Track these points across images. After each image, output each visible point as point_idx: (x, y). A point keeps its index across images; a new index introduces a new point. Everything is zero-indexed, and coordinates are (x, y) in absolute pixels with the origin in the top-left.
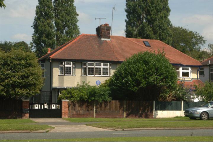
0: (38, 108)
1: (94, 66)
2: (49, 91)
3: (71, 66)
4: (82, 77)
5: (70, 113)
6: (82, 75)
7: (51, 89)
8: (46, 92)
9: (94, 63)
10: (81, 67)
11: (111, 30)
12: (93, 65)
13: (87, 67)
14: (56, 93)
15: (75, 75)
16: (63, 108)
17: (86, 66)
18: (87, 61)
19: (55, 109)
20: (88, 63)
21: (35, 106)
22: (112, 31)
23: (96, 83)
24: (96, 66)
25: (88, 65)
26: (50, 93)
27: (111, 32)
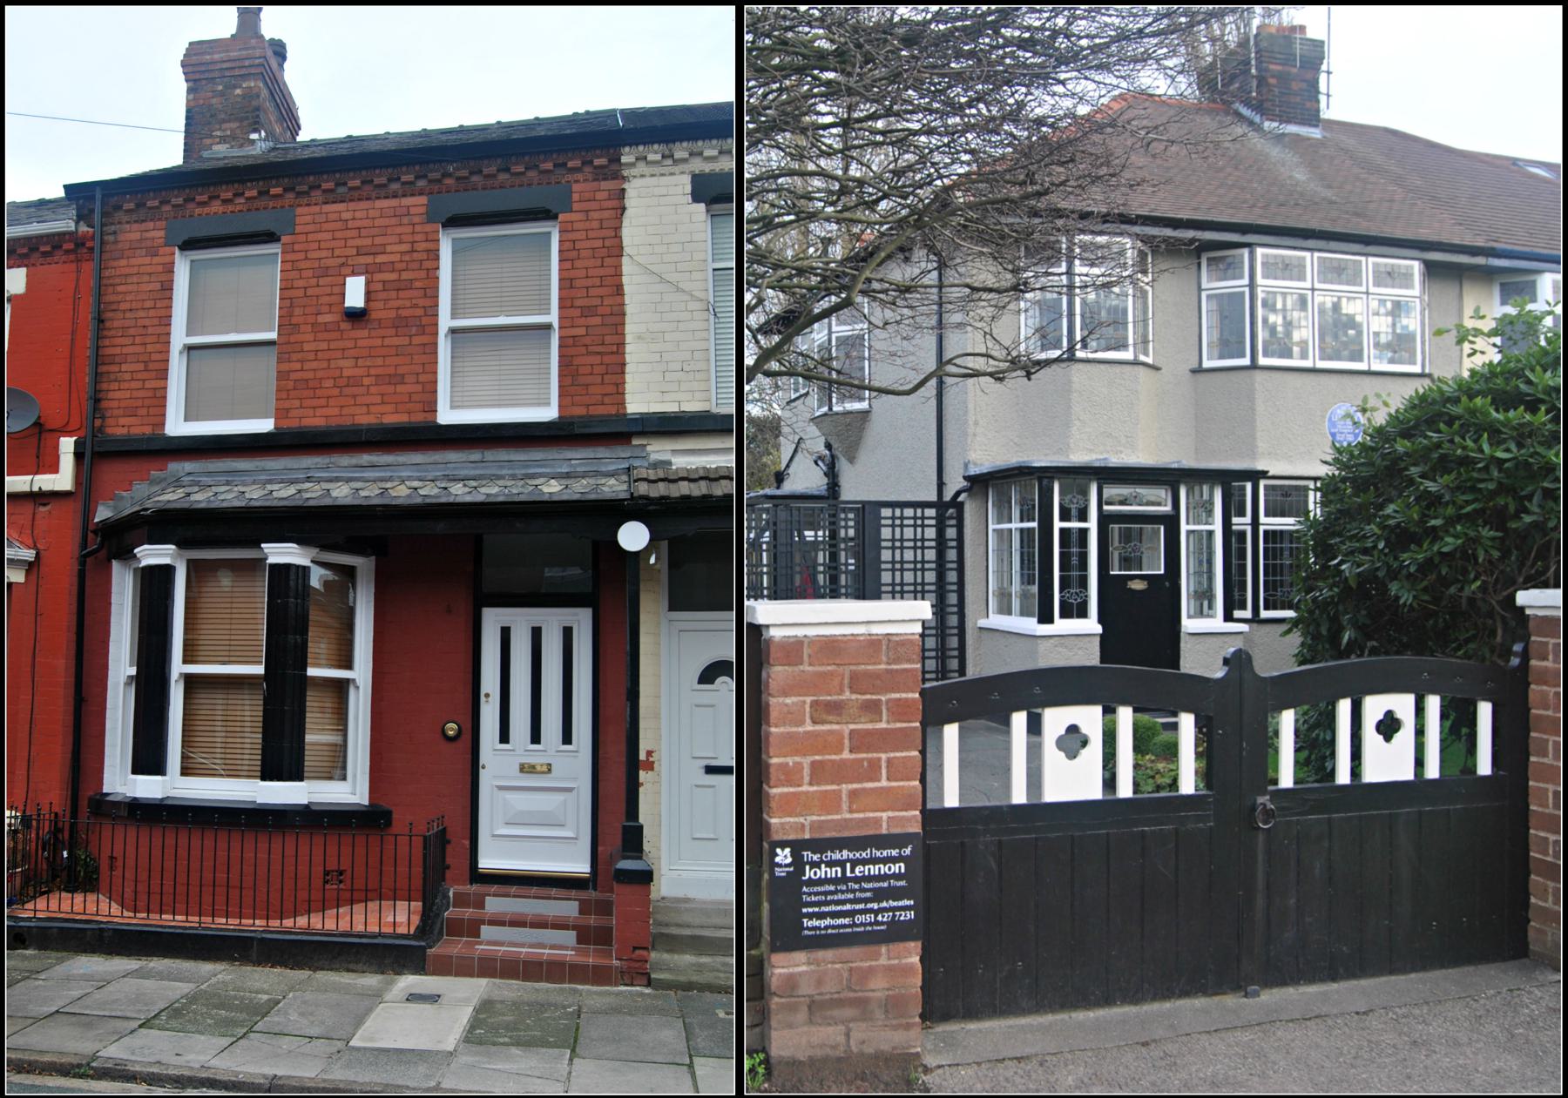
0: (1094, 791)
2: (933, 498)
4: (1202, 377)
6: (1207, 364)
7: (955, 483)
8: (909, 512)
9: (1307, 255)
10: (1200, 289)
11: (1324, 67)
15: (1149, 360)
17: (1246, 281)
19: (1417, 788)
20: (1260, 251)
21: (1035, 727)
22: (1329, 73)
27: (1323, 78)
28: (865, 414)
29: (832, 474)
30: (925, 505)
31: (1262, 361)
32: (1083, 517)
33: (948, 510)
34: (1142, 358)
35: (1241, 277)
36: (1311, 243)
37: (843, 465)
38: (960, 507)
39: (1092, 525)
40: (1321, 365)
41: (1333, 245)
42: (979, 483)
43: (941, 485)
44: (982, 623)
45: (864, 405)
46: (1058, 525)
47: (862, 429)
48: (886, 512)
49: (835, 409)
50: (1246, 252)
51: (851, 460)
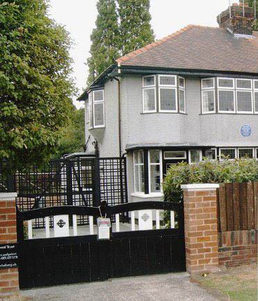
1: (234, 88)
3: (174, 87)
5: (224, 246)
7: (124, 152)
8: (108, 161)
9: (234, 79)
12: (232, 86)
13: (216, 89)
14: (137, 162)
16: (193, 223)
17: (214, 87)
18: (215, 75)
23: (242, 131)
24: (238, 87)
25: (220, 86)
26: (121, 162)
28: (105, 128)
29: (96, 147)
30: (113, 159)
31: (219, 112)
32: (158, 162)
33: (122, 158)
34: (180, 112)
35: (212, 86)
36: (234, 76)
37: (99, 144)
38: (125, 159)
39: (161, 164)
40: (238, 112)
41: (241, 76)
42: (131, 151)
43: (120, 152)
44: (133, 194)
45: (103, 126)
46: (150, 164)
47: (104, 133)
48: (101, 161)
49: (95, 127)
50: (214, 78)
51: (101, 143)
